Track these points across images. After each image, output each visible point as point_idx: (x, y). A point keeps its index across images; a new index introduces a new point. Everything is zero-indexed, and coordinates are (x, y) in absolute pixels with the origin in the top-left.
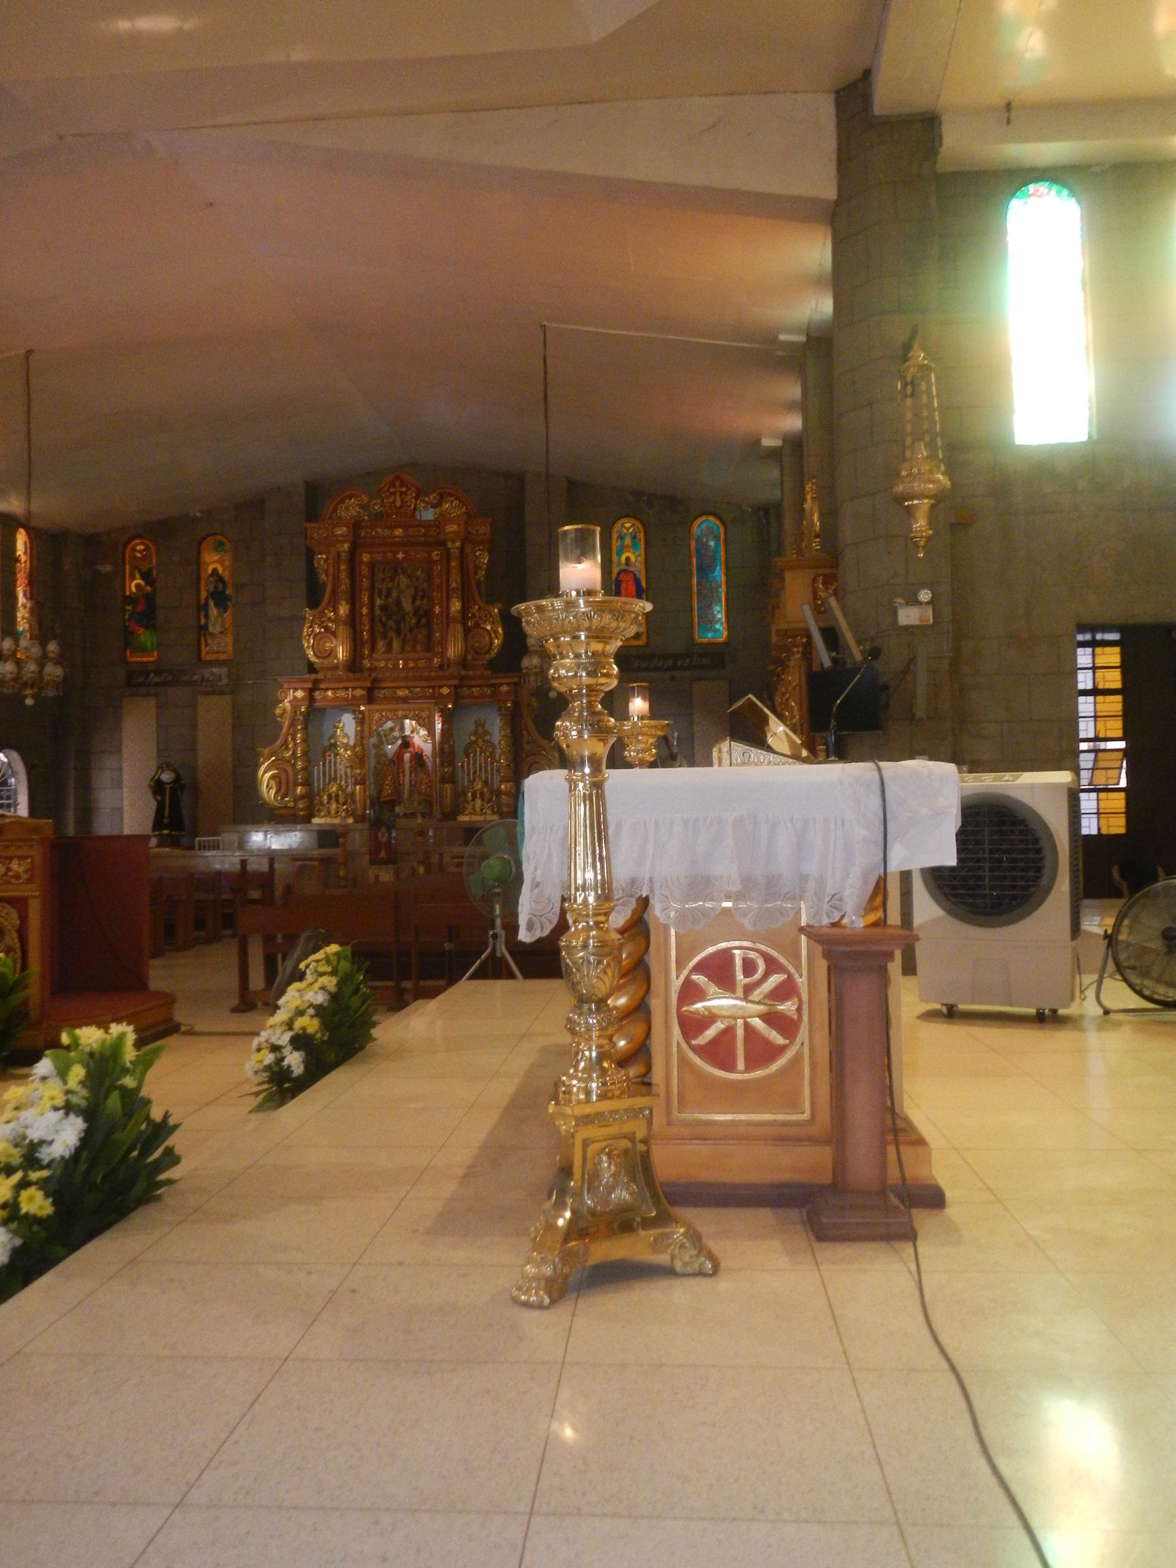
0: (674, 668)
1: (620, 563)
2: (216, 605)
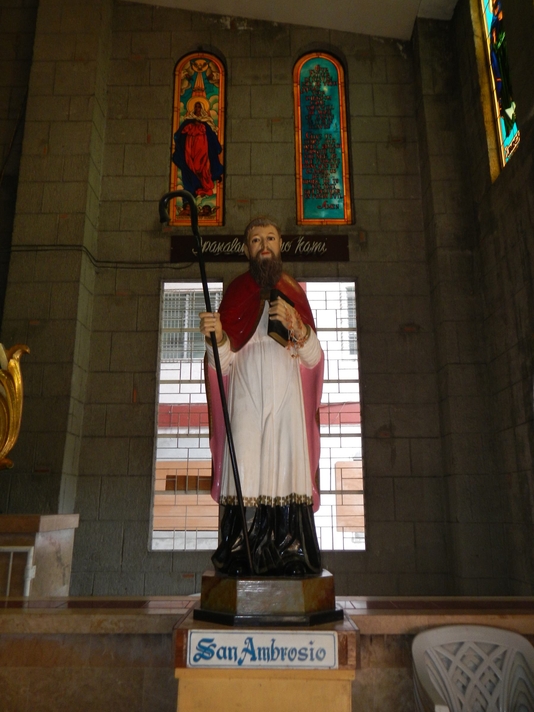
1: (187, 113)
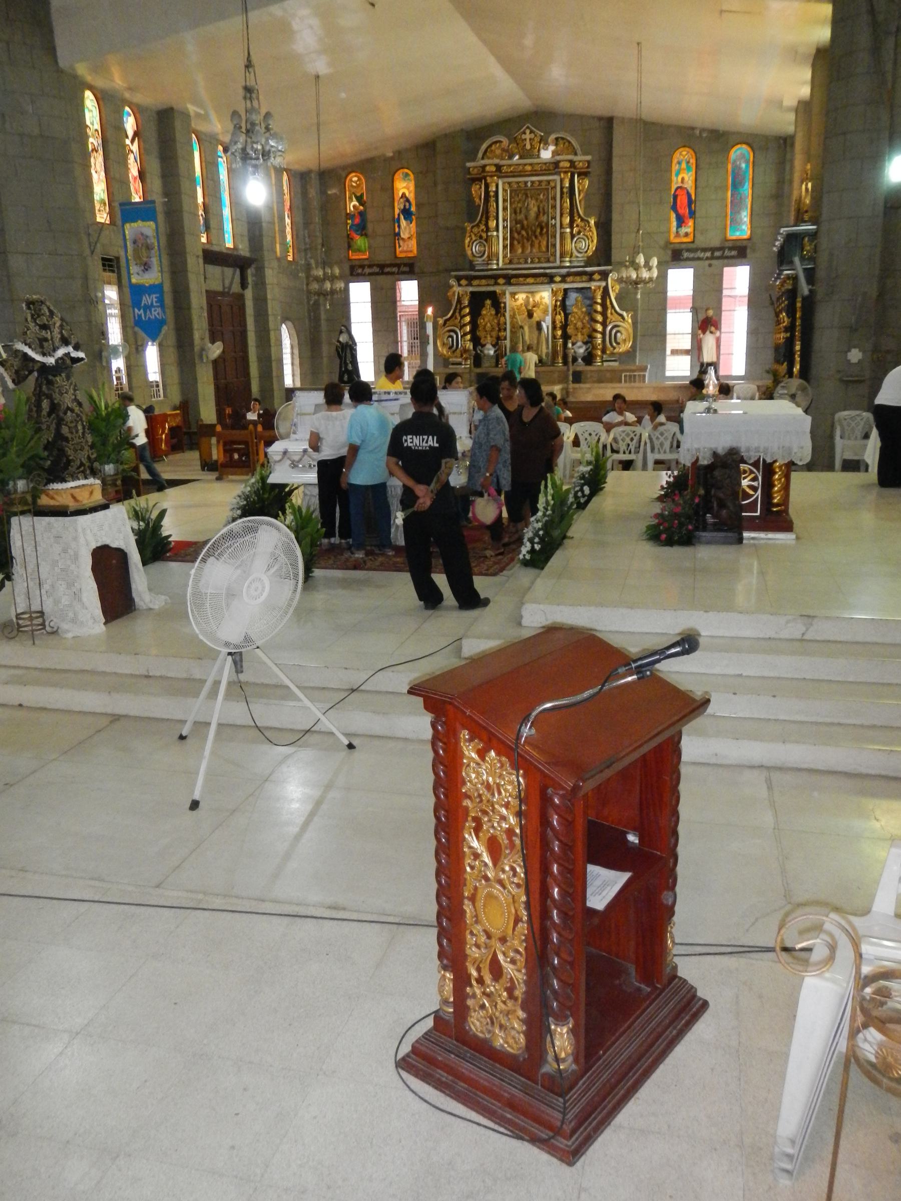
0: (713, 258)
1: (677, 183)
2: (405, 218)
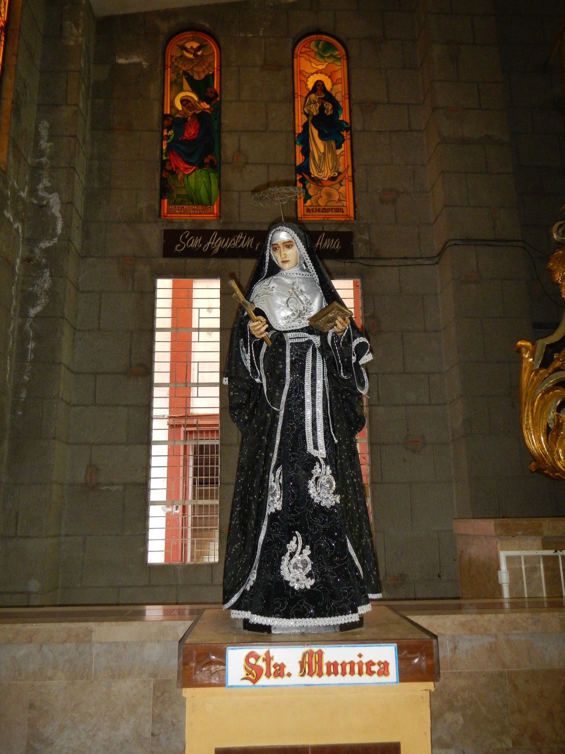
2: (322, 136)
